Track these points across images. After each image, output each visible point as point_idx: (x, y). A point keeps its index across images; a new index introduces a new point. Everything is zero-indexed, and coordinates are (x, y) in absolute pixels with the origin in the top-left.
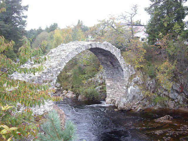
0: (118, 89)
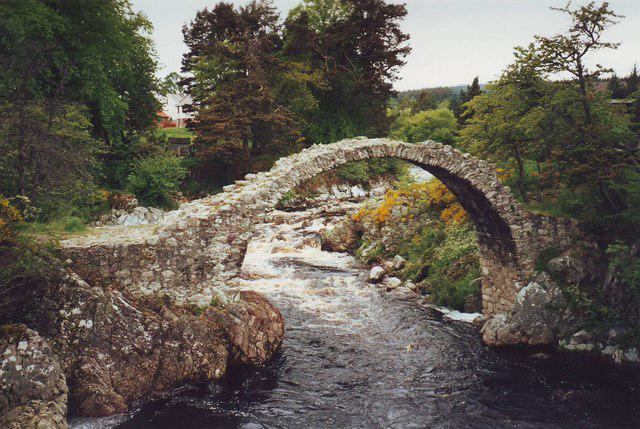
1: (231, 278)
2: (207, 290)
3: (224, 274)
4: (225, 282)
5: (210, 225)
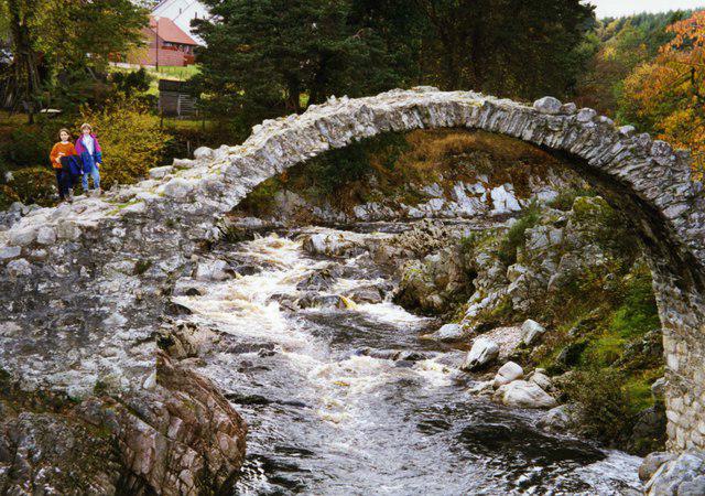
1: (139, 342)
2: (89, 364)
3: (127, 335)
4: (127, 349)
5: (101, 240)
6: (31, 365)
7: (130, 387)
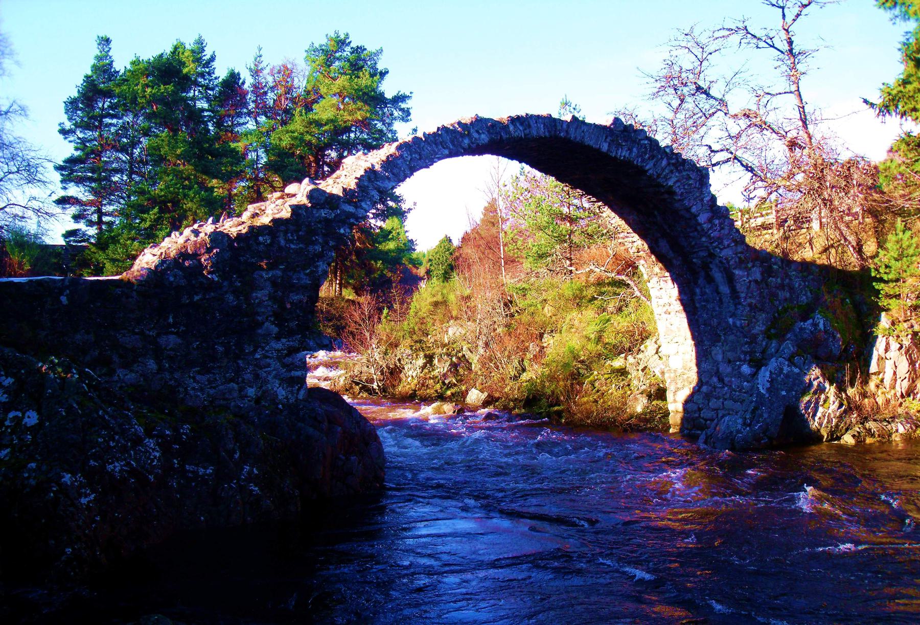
0: (715, 379)
2: (248, 376)
3: (279, 346)
4: (279, 359)
6: (194, 378)
7: (287, 398)
